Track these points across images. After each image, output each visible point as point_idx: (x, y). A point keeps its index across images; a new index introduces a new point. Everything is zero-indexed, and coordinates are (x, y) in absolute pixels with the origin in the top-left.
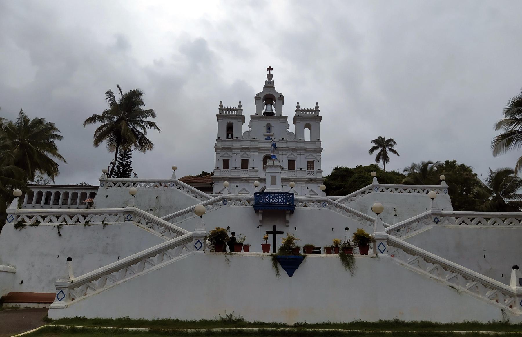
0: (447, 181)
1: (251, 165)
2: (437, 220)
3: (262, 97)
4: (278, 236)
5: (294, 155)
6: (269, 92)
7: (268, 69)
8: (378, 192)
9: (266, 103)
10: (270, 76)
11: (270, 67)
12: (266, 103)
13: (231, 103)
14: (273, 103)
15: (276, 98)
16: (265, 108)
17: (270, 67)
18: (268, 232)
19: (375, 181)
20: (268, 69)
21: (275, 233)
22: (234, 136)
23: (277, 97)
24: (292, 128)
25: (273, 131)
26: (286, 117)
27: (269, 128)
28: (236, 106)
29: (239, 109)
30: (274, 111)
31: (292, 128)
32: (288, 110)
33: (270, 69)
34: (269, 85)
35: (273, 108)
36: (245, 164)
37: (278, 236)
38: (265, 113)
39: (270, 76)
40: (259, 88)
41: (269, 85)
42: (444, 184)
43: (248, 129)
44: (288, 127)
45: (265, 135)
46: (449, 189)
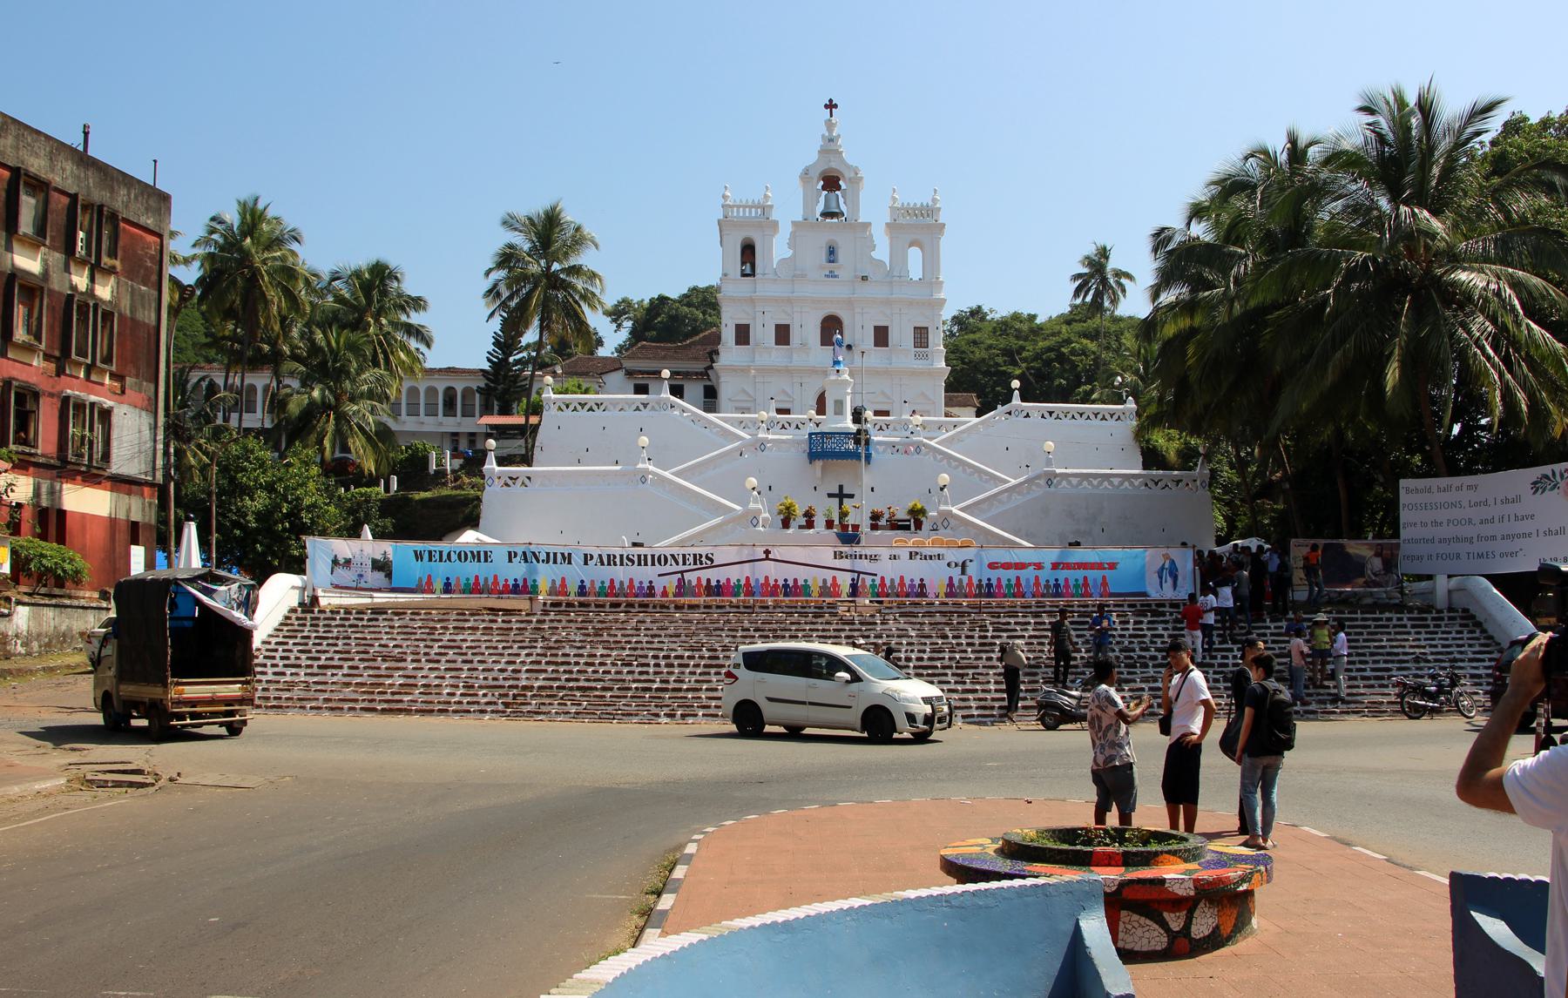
3: (816, 174)
6: (833, 165)
7: (826, 106)
8: (1021, 418)
9: (824, 188)
10: (830, 125)
12: (824, 188)
13: (745, 192)
14: (839, 188)
16: (822, 199)
18: (830, 495)
19: (1016, 400)
20: (826, 106)
21: (841, 495)
22: (758, 271)
23: (848, 174)
24: (882, 252)
25: (842, 255)
26: (867, 225)
28: (758, 197)
29: (765, 209)
30: (844, 208)
31: (882, 252)
32: (872, 206)
33: (831, 106)
34: (830, 145)
35: (841, 200)
39: (830, 125)
40: (809, 155)
41: (830, 145)
43: (789, 253)
44: (873, 248)
45: (821, 267)
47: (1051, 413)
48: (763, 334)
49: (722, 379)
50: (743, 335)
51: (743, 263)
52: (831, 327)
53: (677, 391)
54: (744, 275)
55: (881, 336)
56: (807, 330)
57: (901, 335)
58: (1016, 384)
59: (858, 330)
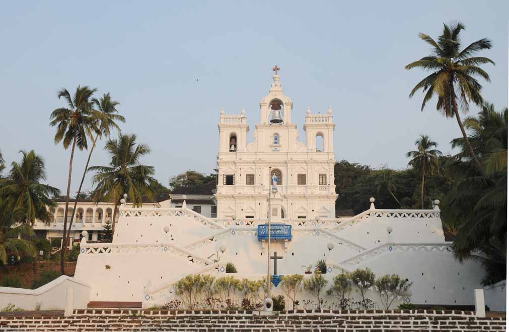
0: (440, 206)
1: (257, 179)
2: (390, 249)
4: (278, 260)
5: (304, 169)
11: (276, 67)
15: (284, 102)
17: (276, 67)
25: (281, 142)
27: (276, 138)
33: (276, 69)
36: (251, 179)
37: (278, 260)
38: (271, 121)
42: (437, 209)
46: (441, 213)
47: (392, 214)
48: (240, 180)
49: (218, 202)
50: (230, 180)
51: (231, 146)
52: (277, 176)
53: (197, 209)
54: (231, 151)
55: (302, 179)
56: (264, 178)
57: (313, 179)
58: (372, 199)
59: (289, 178)
